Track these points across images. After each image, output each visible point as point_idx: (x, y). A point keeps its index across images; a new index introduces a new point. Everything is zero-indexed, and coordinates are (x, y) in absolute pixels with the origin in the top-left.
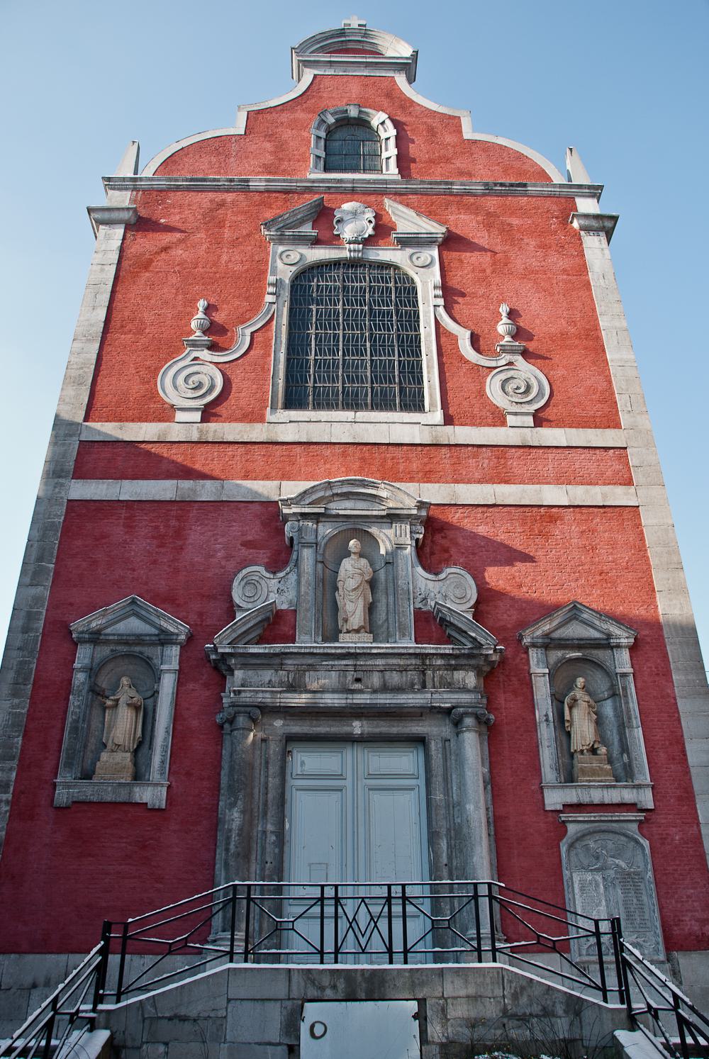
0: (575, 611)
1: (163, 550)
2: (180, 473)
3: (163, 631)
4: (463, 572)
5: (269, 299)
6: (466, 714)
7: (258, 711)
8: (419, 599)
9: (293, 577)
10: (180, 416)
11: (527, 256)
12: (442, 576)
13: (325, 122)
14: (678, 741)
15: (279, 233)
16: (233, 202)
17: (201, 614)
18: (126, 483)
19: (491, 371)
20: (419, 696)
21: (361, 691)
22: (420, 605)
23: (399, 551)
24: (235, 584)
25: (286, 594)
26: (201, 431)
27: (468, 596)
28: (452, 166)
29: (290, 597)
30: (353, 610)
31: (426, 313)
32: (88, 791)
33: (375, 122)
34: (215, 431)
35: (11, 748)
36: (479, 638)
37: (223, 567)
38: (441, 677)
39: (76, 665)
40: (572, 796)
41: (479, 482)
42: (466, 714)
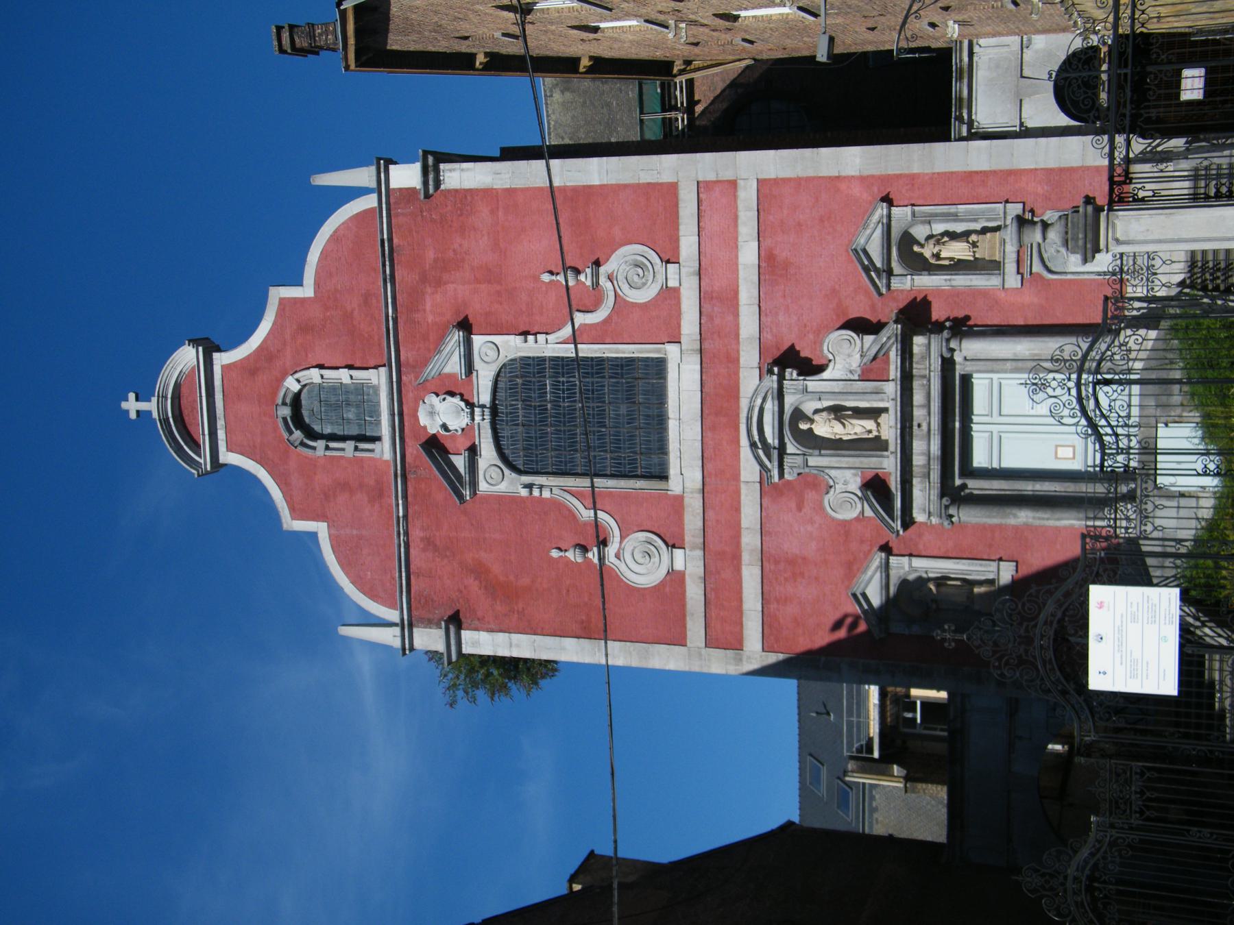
5: (546, 494)
9: (833, 473)
10: (679, 565)
11: (478, 249)
12: (831, 357)
14: (969, 176)
16: (423, 529)
17: (862, 542)
18: (746, 606)
24: (839, 516)
26: (693, 548)
28: (356, 313)
30: (858, 428)
31: (554, 350)
33: (295, 387)
40: (1010, 267)
41: (737, 315)
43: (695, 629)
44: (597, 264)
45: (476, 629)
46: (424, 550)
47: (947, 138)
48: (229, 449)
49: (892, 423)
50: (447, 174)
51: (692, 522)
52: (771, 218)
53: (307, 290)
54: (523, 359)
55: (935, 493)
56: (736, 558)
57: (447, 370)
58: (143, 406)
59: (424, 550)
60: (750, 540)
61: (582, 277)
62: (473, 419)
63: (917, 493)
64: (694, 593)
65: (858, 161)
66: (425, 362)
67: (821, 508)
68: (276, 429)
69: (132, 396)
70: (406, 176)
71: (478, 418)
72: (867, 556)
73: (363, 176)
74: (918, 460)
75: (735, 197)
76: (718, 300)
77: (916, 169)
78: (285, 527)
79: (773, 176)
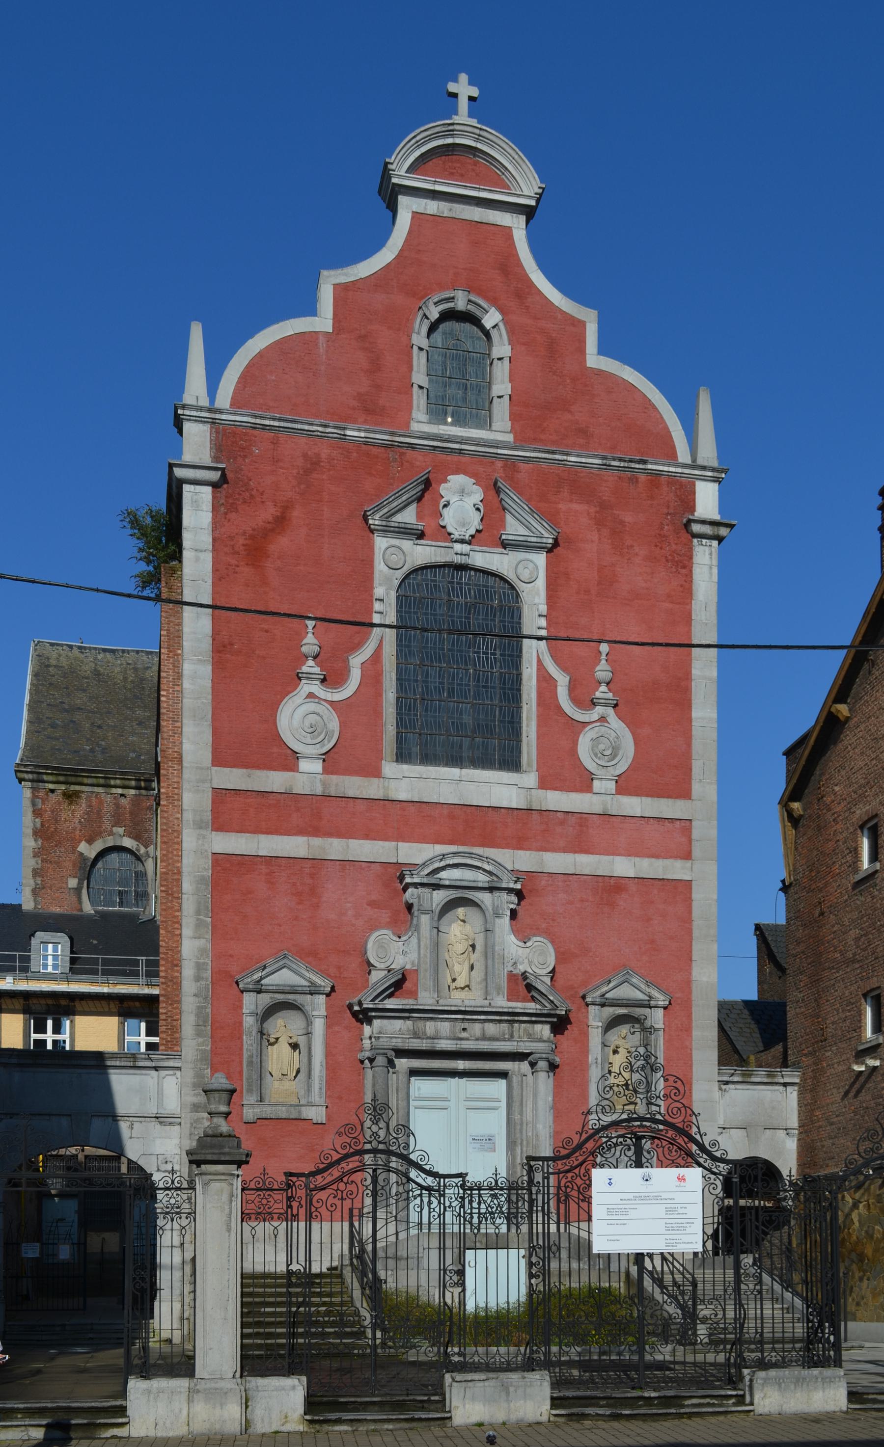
0: (627, 976)
1: (300, 907)
2: (310, 829)
3: (313, 984)
4: (545, 941)
6: (541, 1059)
7: (393, 1054)
8: (511, 964)
9: (414, 940)
12: (528, 944)
13: (427, 318)
15: (384, 523)
17: (339, 968)
18: (262, 838)
19: (584, 727)
20: (508, 1043)
21: (467, 1039)
22: (511, 969)
23: (497, 920)
24: (370, 945)
25: (409, 956)
26: (324, 784)
27: (548, 963)
29: (412, 959)
32: (267, 1111)
34: (337, 785)
35: (203, 1078)
36: (555, 1001)
37: (353, 925)
38: (525, 1029)
39: (244, 1011)
42: (541, 1059)
43: (233, 778)
44: (615, 706)
45: (215, 509)
46: (305, 456)
47: (720, 1063)
48: (417, 216)
49: (467, 1003)
50: (707, 549)
51: (354, 786)
52: (656, 892)
53: (594, 360)
54: (519, 610)
55: (399, 1044)
56: (314, 830)
57: (509, 518)
58: (463, 104)
59: (305, 456)
60: (335, 848)
61: (603, 688)
62: (456, 541)
63: (398, 1024)
64: (274, 781)
65: (705, 979)
66: (520, 493)
67: (374, 928)
68: (442, 287)
69: (475, 92)
70: (707, 500)
71: (458, 547)
72: (325, 974)
73: (708, 453)
74: (430, 1027)
75: (676, 857)
76: (580, 832)
77: (696, 1033)
78: (325, 273)
79: (694, 896)
